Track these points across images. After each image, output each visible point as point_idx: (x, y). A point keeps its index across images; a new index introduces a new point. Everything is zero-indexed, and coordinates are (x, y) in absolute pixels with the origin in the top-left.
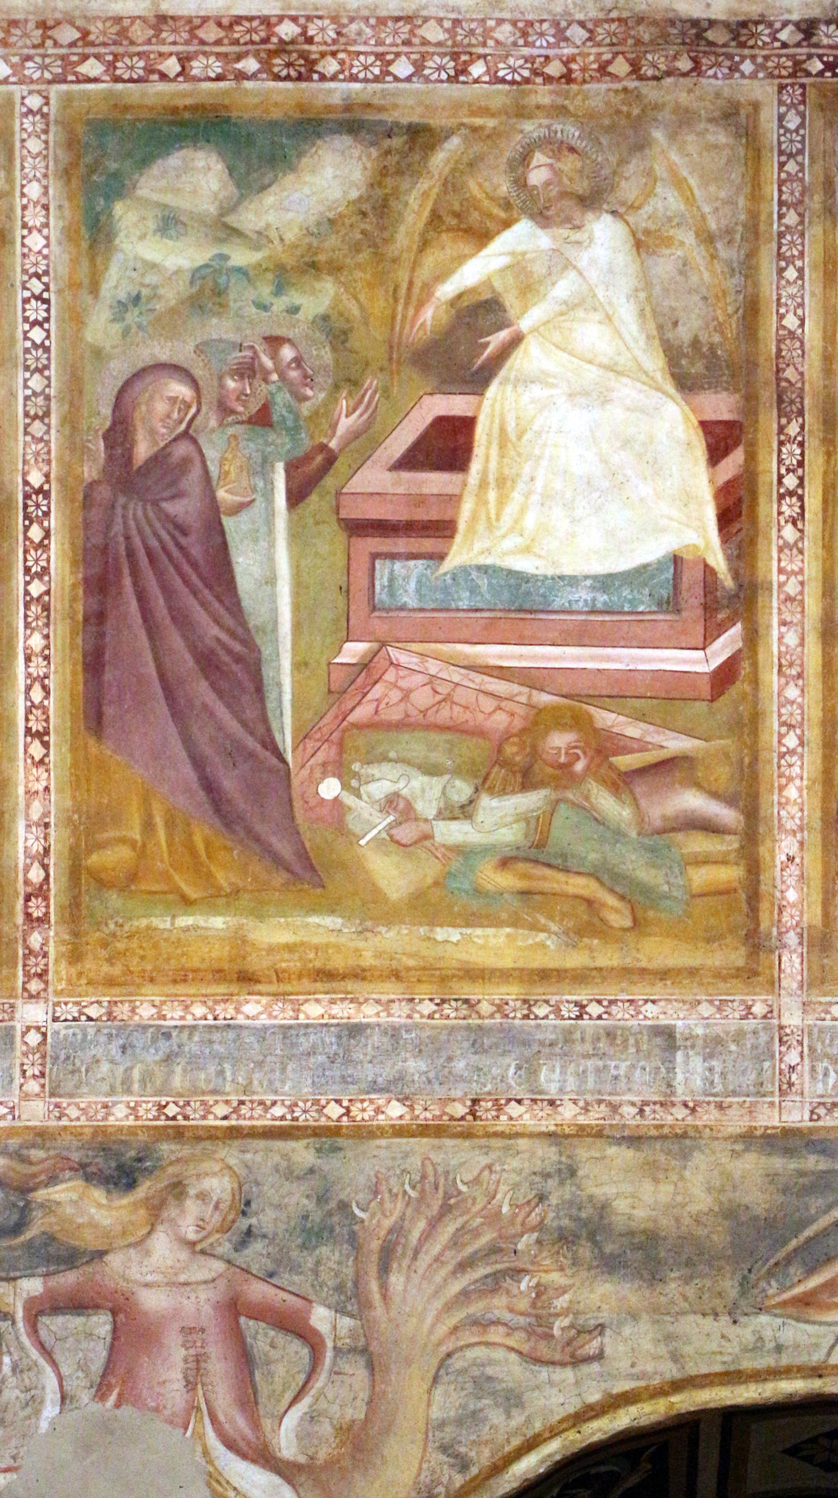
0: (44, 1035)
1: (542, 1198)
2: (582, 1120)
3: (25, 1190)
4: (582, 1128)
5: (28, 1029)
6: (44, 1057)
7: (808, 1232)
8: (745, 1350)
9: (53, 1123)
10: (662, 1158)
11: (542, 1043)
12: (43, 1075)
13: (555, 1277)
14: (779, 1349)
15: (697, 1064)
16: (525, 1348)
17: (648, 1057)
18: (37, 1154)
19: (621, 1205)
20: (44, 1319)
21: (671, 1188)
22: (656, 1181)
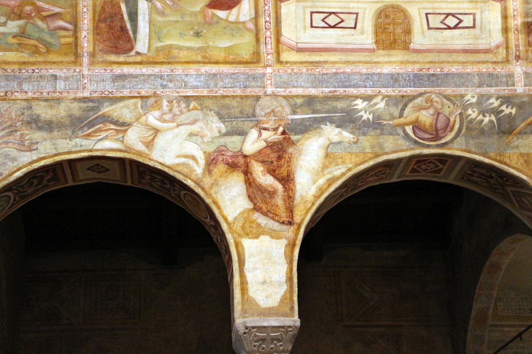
1: (23, 114)
2: (33, 96)
4: (33, 98)
7: (89, 120)
8: (73, 146)
10: (53, 104)
11: (23, 79)
13: (26, 132)
14: (81, 146)
15: (62, 83)
16: (18, 148)
17: (50, 81)
19: (43, 115)
21: (55, 111)
22: (52, 109)
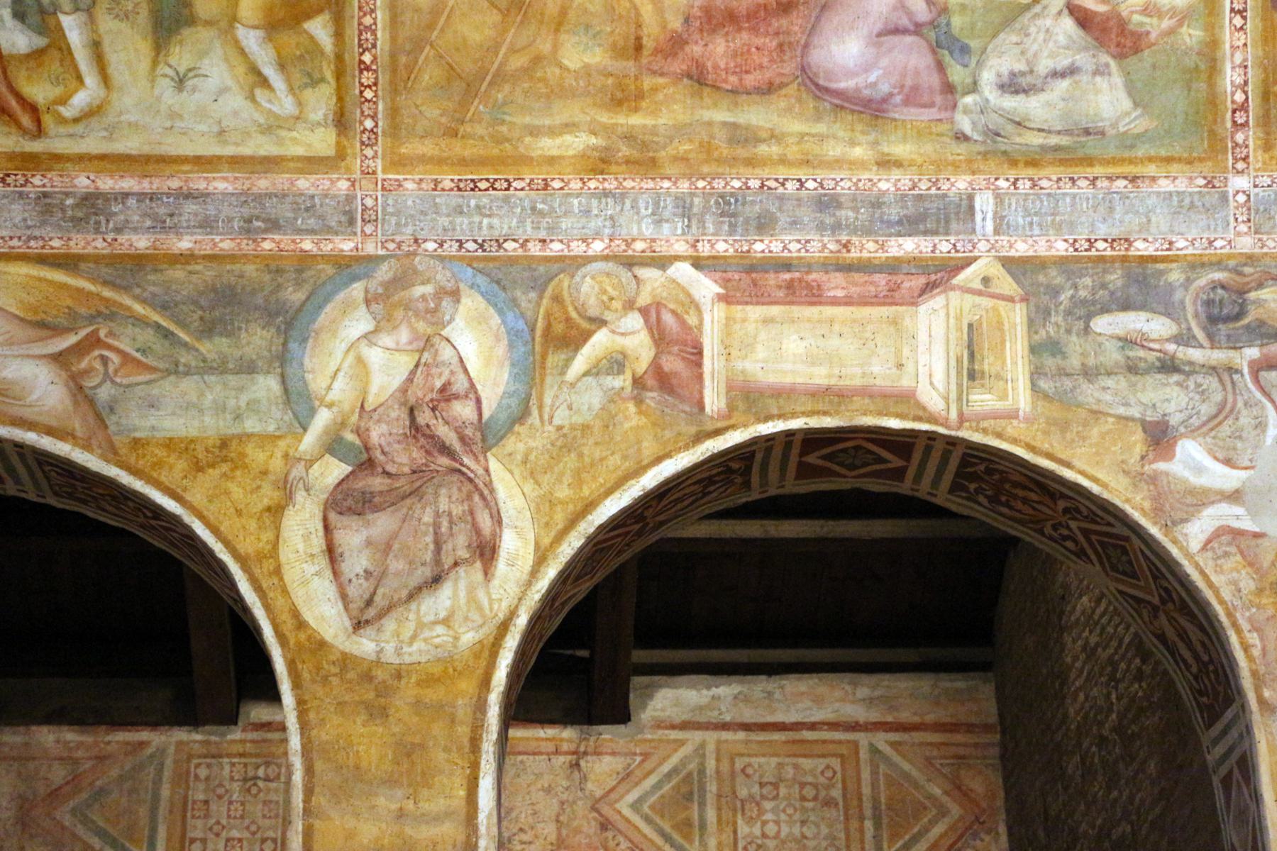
0: (1249, 196)
3: (1242, 292)
5: (1238, 192)
6: (1249, 209)
9: (1257, 250)
12: (1249, 220)
18: (1247, 270)
20: (1263, 374)
